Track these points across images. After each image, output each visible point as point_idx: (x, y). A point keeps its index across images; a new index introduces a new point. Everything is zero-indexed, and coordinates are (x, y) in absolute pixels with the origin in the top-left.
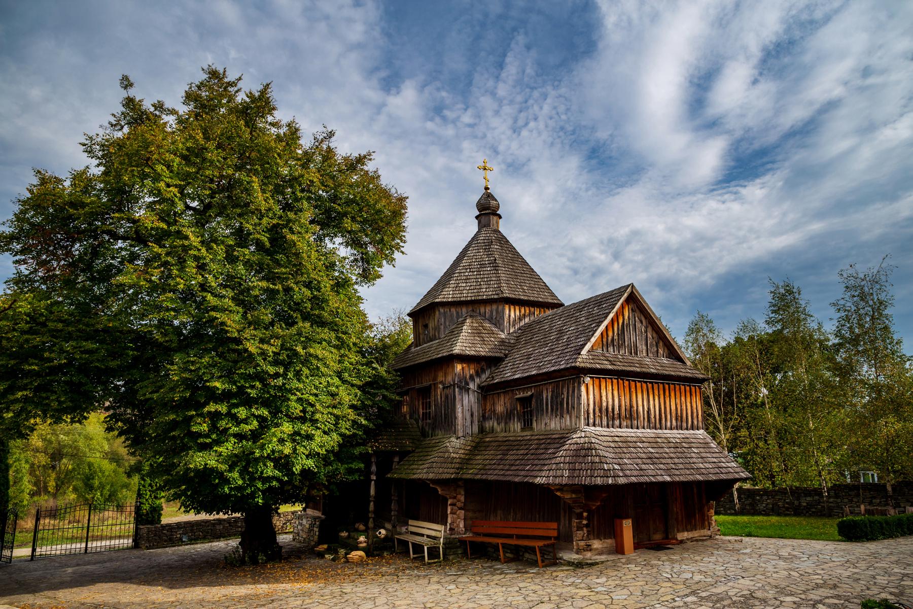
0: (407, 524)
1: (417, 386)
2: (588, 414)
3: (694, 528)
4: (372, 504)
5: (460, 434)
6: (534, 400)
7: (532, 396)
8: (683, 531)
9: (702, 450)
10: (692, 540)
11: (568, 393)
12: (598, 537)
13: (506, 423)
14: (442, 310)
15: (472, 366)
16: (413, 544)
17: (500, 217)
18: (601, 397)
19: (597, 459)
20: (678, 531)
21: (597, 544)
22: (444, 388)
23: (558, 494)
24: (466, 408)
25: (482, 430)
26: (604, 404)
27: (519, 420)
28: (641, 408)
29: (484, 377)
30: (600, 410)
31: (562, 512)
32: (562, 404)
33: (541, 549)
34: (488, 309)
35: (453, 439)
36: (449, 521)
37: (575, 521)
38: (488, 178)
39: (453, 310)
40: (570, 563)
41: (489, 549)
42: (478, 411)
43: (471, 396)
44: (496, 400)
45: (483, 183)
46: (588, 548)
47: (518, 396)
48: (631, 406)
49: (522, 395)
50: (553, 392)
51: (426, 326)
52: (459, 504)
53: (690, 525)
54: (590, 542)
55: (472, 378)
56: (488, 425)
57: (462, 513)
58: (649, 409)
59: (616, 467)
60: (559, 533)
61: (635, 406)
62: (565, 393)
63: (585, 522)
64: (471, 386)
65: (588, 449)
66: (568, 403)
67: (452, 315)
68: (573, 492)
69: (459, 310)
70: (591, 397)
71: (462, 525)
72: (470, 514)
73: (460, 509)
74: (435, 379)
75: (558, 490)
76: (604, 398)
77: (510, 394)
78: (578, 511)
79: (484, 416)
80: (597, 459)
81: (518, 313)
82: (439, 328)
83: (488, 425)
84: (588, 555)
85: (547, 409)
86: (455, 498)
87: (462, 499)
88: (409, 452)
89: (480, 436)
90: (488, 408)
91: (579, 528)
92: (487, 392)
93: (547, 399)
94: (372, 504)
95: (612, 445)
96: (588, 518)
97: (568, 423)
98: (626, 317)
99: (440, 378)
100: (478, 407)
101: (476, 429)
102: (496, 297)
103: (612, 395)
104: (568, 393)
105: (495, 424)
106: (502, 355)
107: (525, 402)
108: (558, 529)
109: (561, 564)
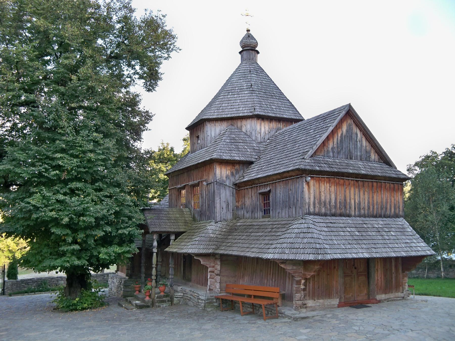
1: (191, 183)
4: (154, 270)
5: (218, 219)
7: (270, 191)
8: (382, 293)
9: (399, 234)
10: (388, 300)
13: (252, 212)
15: (229, 168)
17: (258, 52)
19: (312, 241)
20: (378, 294)
21: (310, 303)
22: (207, 185)
23: (282, 266)
24: (223, 199)
25: (236, 217)
26: (323, 198)
28: (353, 202)
30: (320, 203)
35: (213, 223)
36: (209, 284)
40: (289, 317)
46: (304, 306)
47: (261, 191)
48: (345, 200)
53: (387, 289)
54: (306, 302)
56: (241, 213)
59: (327, 246)
61: (348, 201)
63: (302, 287)
72: (225, 279)
73: (217, 275)
75: (282, 263)
76: (322, 194)
78: (298, 279)
79: (237, 207)
80: (312, 241)
83: (241, 213)
84: (304, 310)
86: (213, 267)
87: (218, 267)
88: (184, 232)
89: (234, 221)
91: (297, 292)
92: (239, 187)
94: (154, 270)
95: (326, 229)
96: (305, 285)
99: (205, 178)
101: (230, 216)
102: (251, 114)
103: (327, 191)
105: (245, 212)
106: (254, 160)
109: (283, 317)
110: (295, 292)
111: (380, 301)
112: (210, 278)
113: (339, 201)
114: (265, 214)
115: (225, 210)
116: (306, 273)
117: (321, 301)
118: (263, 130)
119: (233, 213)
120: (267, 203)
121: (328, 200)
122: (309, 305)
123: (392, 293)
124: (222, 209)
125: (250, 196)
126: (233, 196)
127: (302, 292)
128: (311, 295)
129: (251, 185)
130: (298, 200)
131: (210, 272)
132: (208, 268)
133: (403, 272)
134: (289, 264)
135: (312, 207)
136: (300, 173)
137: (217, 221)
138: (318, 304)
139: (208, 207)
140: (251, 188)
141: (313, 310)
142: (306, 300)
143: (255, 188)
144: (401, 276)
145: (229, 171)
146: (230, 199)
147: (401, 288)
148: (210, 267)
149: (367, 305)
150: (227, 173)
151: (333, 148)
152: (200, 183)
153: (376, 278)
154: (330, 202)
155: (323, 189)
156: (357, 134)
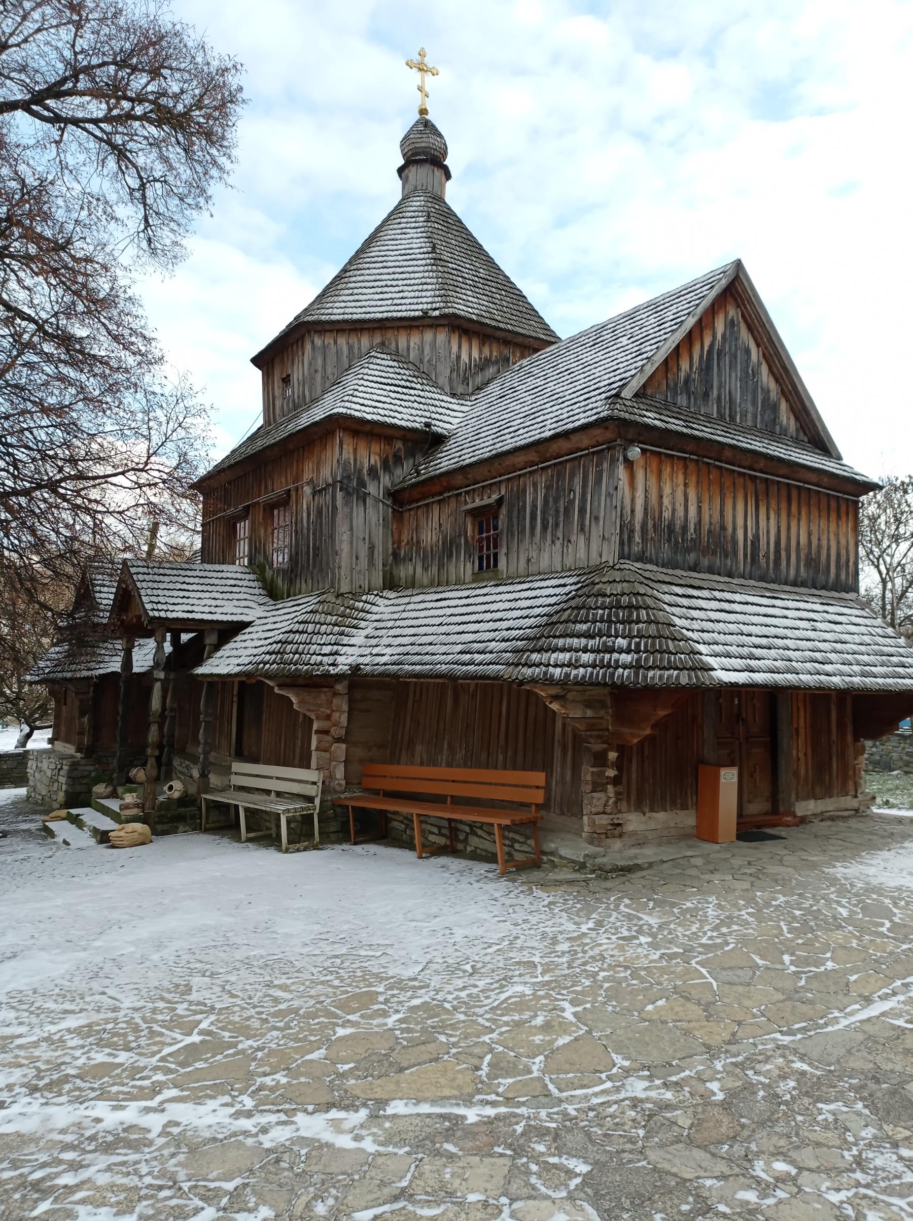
0: (227, 771)
1: (262, 499)
2: (632, 531)
3: (828, 793)
4: (154, 728)
6: (504, 511)
7: (500, 501)
11: (584, 486)
12: (639, 807)
13: (441, 566)
14: (318, 341)
15: (375, 447)
16: (247, 810)
18: (661, 497)
21: (634, 822)
22: (314, 494)
23: (555, 706)
26: (667, 515)
27: (469, 554)
29: (399, 473)
31: (558, 752)
32: (568, 511)
33: (503, 828)
34: (415, 339)
37: (588, 772)
38: (427, 88)
39: (342, 341)
41: (395, 824)
42: (385, 544)
43: (370, 510)
44: (423, 521)
45: (417, 100)
46: (616, 830)
47: (470, 506)
48: (723, 528)
49: (478, 503)
50: (548, 488)
51: (286, 380)
52: (336, 732)
55: (373, 472)
57: (340, 749)
58: (757, 537)
60: (548, 798)
61: (730, 529)
62: (578, 489)
63: (611, 773)
64: (372, 488)
65: (630, 607)
66: (582, 511)
67: (338, 353)
68: (588, 704)
69: (353, 340)
70: (640, 494)
71: (340, 773)
72: (359, 752)
73: (339, 740)
74: (297, 479)
75: (555, 698)
76: (666, 501)
77: (453, 503)
78: (598, 747)
79: (395, 555)
81: (475, 354)
82: (312, 379)
84: (617, 844)
85: (533, 528)
86: (328, 717)
87: (344, 719)
90: (405, 538)
91: (598, 786)
92: (402, 501)
93: (535, 500)
96: (618, 765)
97: (582, 553)
98: (719, 336)
99: (307, 476)
100: (385, 535)
104: (584, 486)
105: (419, 570)
107: (484, 517)
108: (547, 788)
109: (554, 866)
110: (589, 788)
111: (803, 821)
112: (317, 749)
113: (707, 527)
114: (481, 568)
115: (364, 562)
116: (626, 730)
117: (661, 816)
118: (465, 357)
119: (384, 573)
120: (488, 538)
121: (678, 524)
122: (630, 827)
123: (830, 797)
124: (357, 558)
125: (436, 525)
126: (385, 526)
127: (610, 788)
128: (633, 797)
129: (441, 494)
130: (597, 518)
131: (317, 732)
132: (311, 721)
133: (856, 740)
134: (574, 701)
135: (637, 539)
136: (609, 435)
137: (342, 591)
138: (652, 825)
139: (316, 555)
140: (439, 502)
141: (639, 845)
142: (620, 812)
143: (453, 500)
144: (851, 751)
145: (377, 458)
146: (379, 536)
147: (851, 784)
148: (318, 718)
149: (769, 831)
150: (372, 462)
151: (687, 380)
152: (293, 494)
153: (795, 752)
154: (685, 528)
155: (667, 490)
156: (748, 351)
